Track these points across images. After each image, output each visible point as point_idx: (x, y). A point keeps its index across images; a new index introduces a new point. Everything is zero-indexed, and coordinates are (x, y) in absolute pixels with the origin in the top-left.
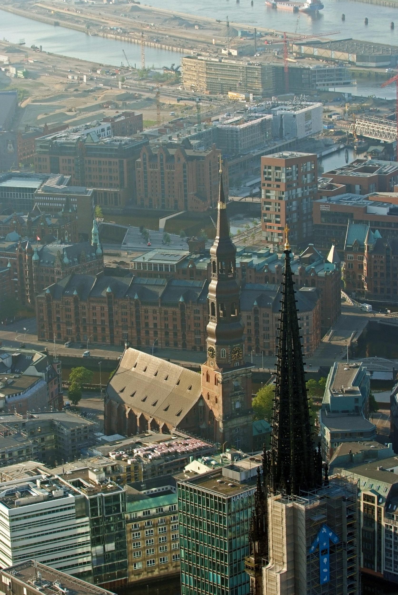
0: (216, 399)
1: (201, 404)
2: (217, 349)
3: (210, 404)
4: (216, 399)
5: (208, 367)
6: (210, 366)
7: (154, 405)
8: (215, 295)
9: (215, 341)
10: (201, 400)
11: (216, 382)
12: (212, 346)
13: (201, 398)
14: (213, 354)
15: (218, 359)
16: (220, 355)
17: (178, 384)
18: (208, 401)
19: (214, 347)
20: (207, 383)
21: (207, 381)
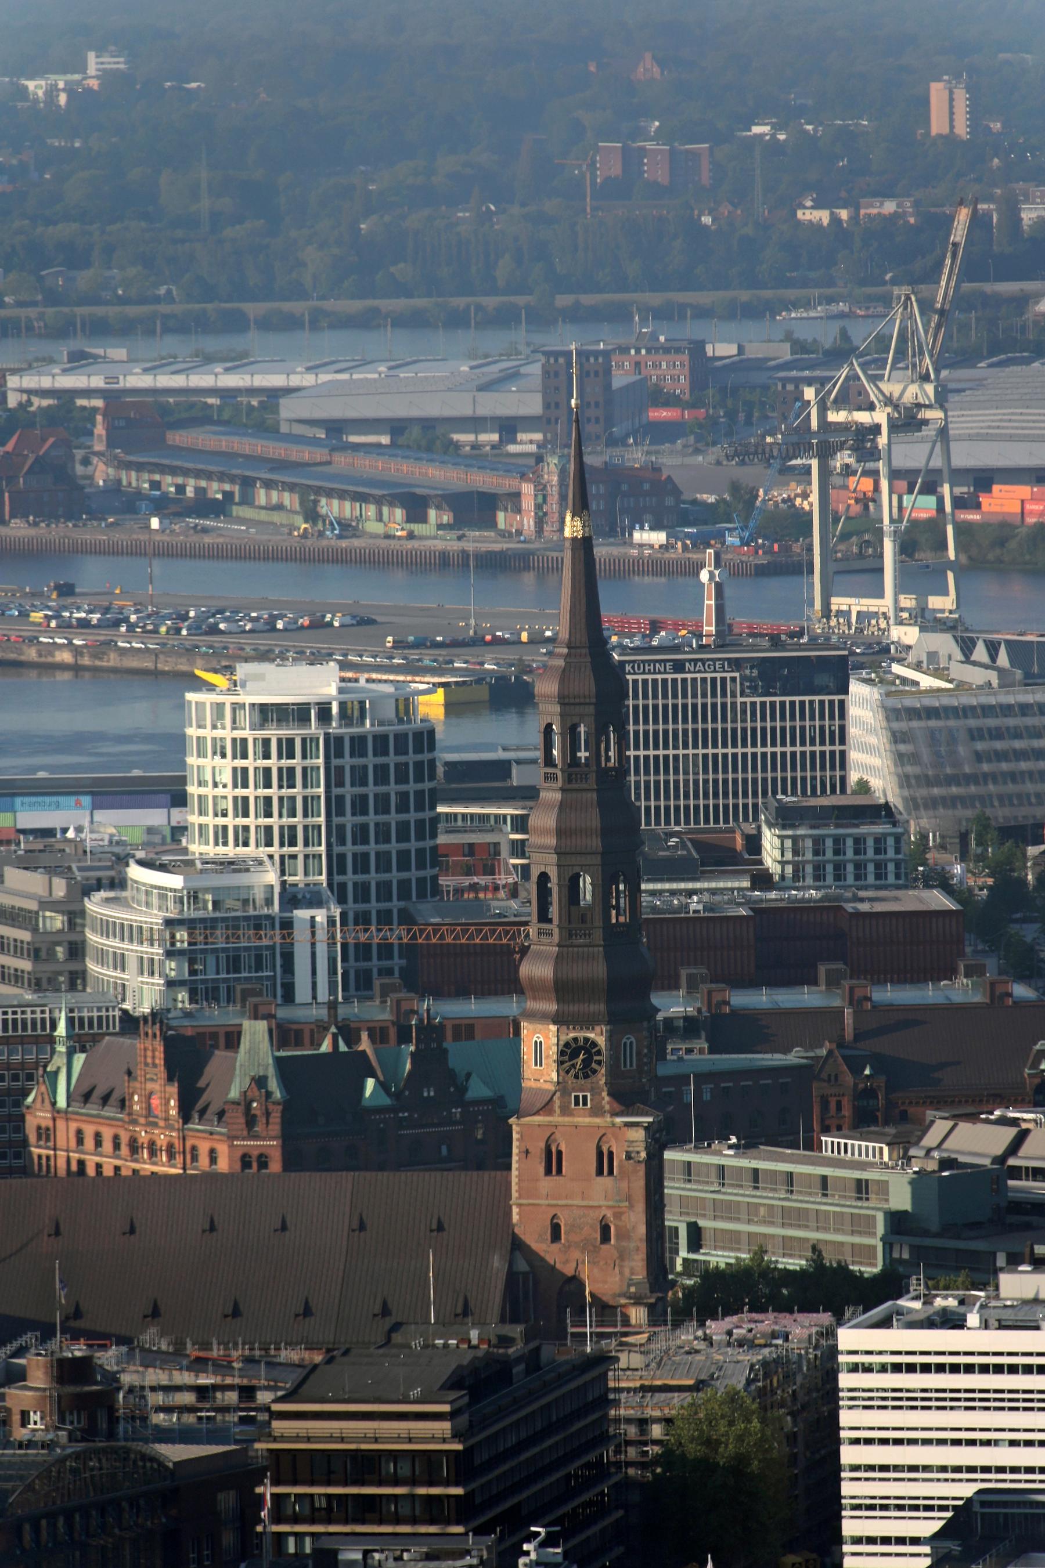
0: (605, 1230)
1: (522, 1266)
2: (610, 1039)
3: (561, 1258)
4: (605, 1230)
5: (557, 1119)
6: (565, 1111)
7: (307, 1312)
8: (596, 843)
9: (600, 1007)
10: (518, 1254)
11: (604, 1163)
12: (581, 1034)
13: (517, 1245)
14: (587, 1062)
15: (614, 1074)
16: (618, 1059)
17: (362, 1227)
18: (555, 1247)
19: (598, 1036)
20: (554, 1179)
21: (548, 1172)
